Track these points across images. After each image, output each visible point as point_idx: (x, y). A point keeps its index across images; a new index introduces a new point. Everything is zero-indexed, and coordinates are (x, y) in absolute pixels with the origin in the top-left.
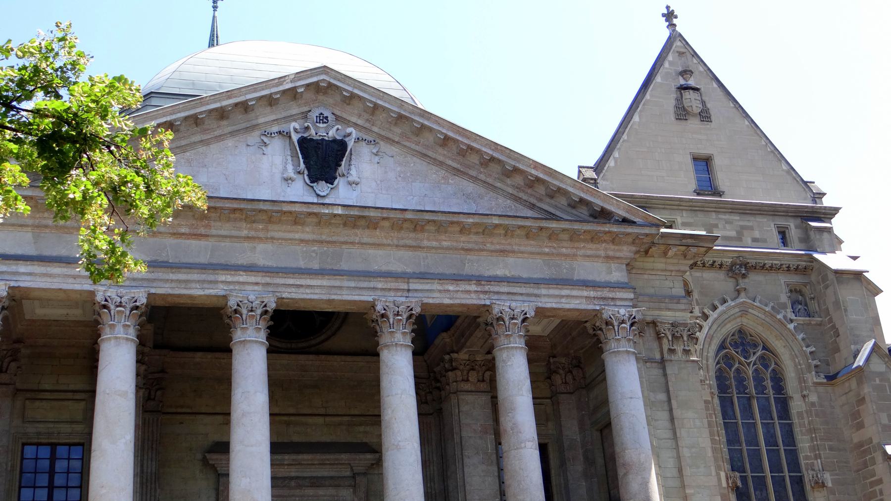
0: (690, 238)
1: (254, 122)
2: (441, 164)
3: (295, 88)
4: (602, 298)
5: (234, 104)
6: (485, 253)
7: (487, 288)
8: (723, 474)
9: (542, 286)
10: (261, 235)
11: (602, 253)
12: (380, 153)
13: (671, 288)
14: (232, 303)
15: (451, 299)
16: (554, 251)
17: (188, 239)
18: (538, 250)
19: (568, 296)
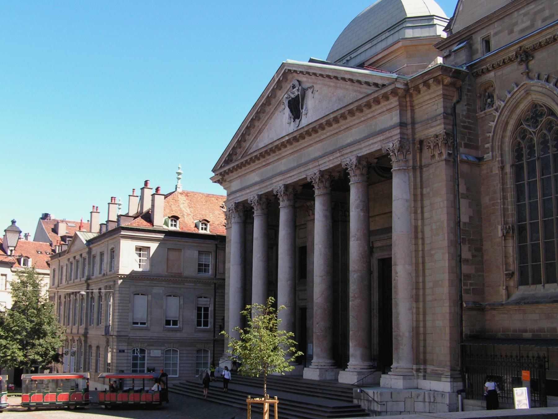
0: (427, 75)
1: (279, 101)
2: (329, 86)
3: (279, 79)
4: (386, 138)
5: (266, 98)
6: (342, 132)
7: (342, 153)
8: (500, 227)
9: (362, 142)
10: (280, 157)
11: (385, 109)
12: (314, 92)
13: (436, 110)
14: (275, 193)
15: (332, 164)
16: (366, 118)
17: (267, 166)
18: (359, 121)
19: (372, 144)
